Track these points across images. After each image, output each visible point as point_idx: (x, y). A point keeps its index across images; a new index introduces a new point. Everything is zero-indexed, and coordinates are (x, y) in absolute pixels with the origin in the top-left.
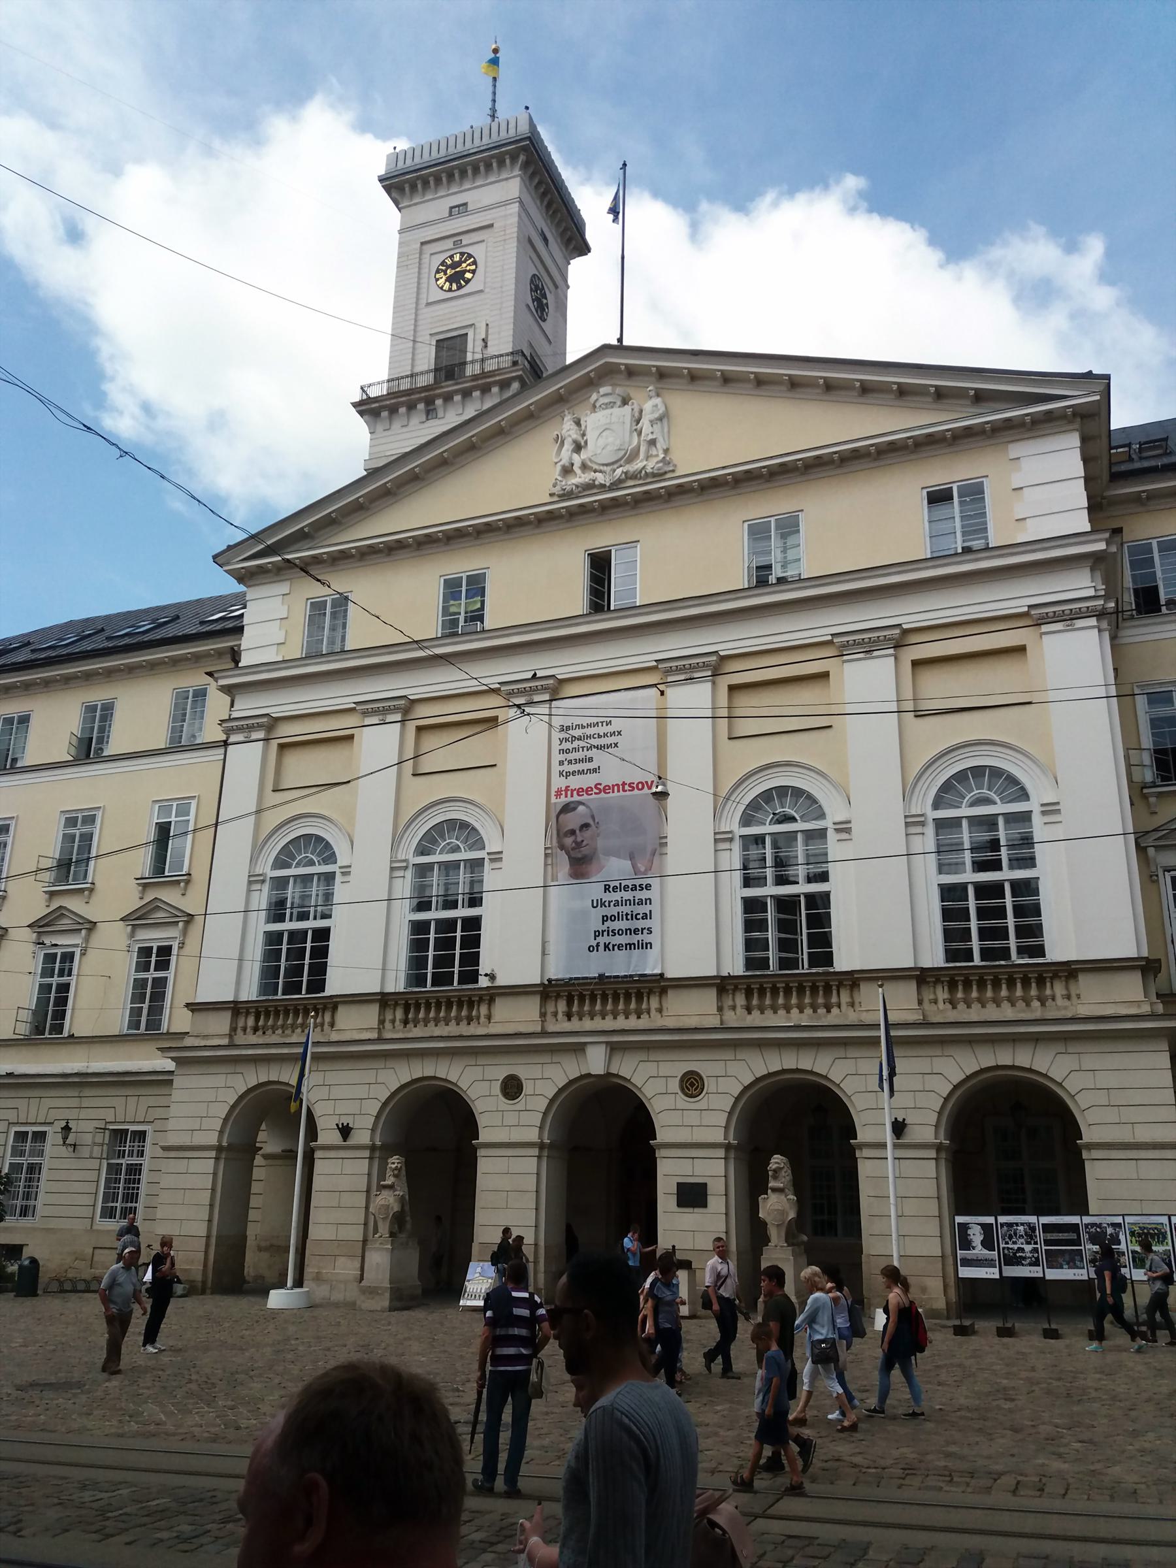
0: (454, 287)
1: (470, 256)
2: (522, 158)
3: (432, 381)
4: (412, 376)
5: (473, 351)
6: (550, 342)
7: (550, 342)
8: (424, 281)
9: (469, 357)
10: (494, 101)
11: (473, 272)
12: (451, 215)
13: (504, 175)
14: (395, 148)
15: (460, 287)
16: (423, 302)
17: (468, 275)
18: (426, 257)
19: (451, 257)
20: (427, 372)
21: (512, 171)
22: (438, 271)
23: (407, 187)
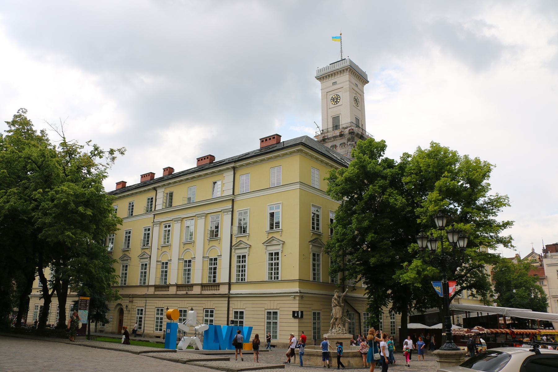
1: (338, 95)
2: (349, 70)
6: (360, 111)
7: (360, 111)
8: (328, 102)
10: (341, 48)
11: (340, 99)
13: (345, 74)
16: (328, 108)
17: (338, 101)
18: (328, 96)
21: (346, 73)
23: (322, 79)
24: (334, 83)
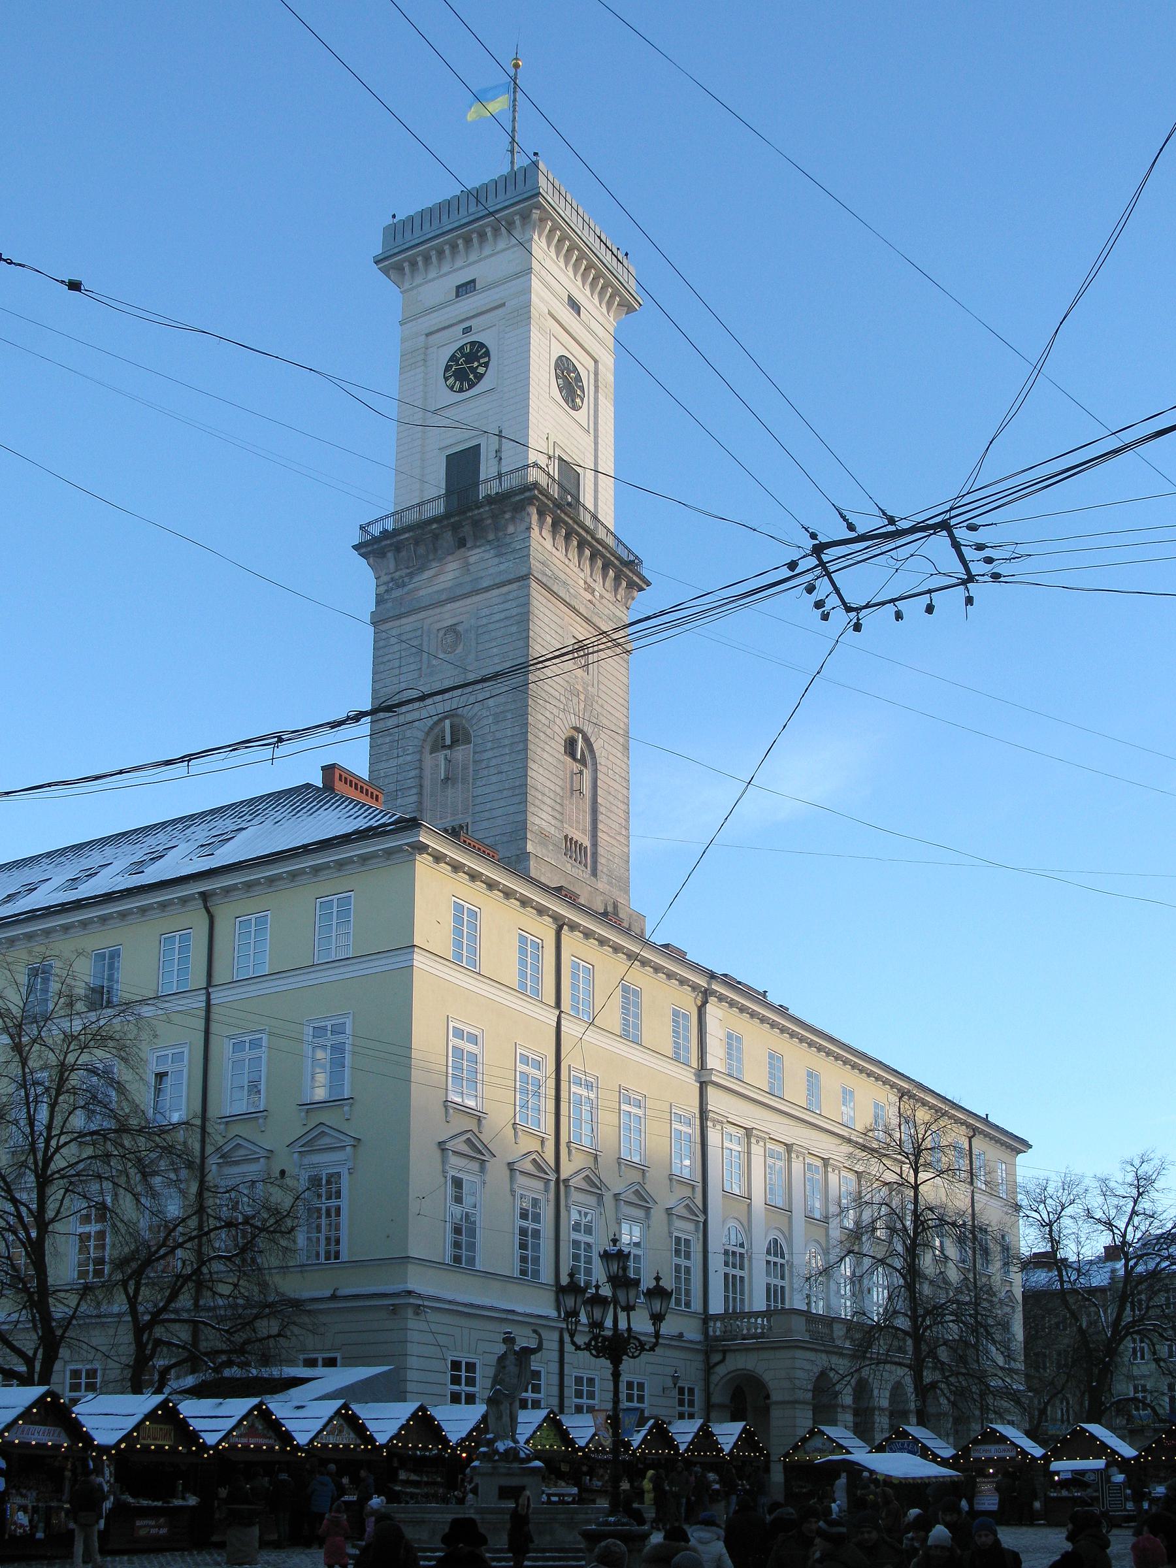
0: (466, 385)
3: (442, 510)
4: (419, 505)
5: (487, 469)
9: (482, 477)
12: (457, 296)
14: (394, 216)
15: (471, 387)
19: (461, 349)
20: (439, 497)
22: (447, 368)
24: (466, 288)
